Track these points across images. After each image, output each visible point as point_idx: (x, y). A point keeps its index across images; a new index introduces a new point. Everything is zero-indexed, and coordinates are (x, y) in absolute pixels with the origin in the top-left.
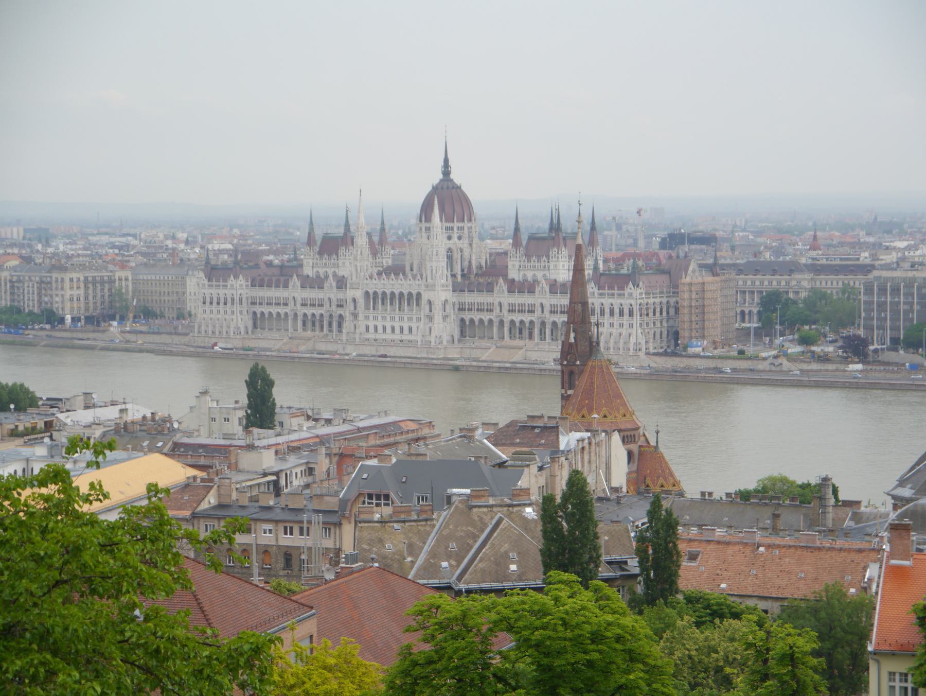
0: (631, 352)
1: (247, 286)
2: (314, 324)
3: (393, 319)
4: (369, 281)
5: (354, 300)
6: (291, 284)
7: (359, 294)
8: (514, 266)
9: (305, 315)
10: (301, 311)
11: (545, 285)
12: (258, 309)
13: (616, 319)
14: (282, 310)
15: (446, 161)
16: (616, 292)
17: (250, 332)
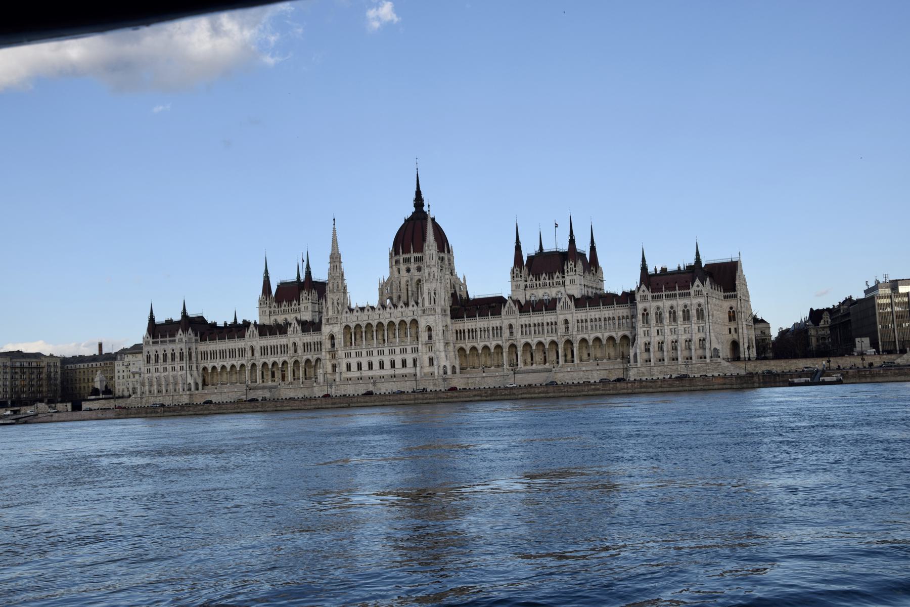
0: (708, 360)
1: (196, 340)
2: (273, 375)
3: (381, 353)
4: (349, 314)
5: (332, 337)
6: (247, 334)
7: (337, 330)
8: (518, 287)
9: (265, 364)
10: (260, 360)
11: (568, 299)
12: (209, 365)
13: (681, 325)
14: (237, 362)
15: (418, 193)
16: (677, 292)
17: (200, 387)
